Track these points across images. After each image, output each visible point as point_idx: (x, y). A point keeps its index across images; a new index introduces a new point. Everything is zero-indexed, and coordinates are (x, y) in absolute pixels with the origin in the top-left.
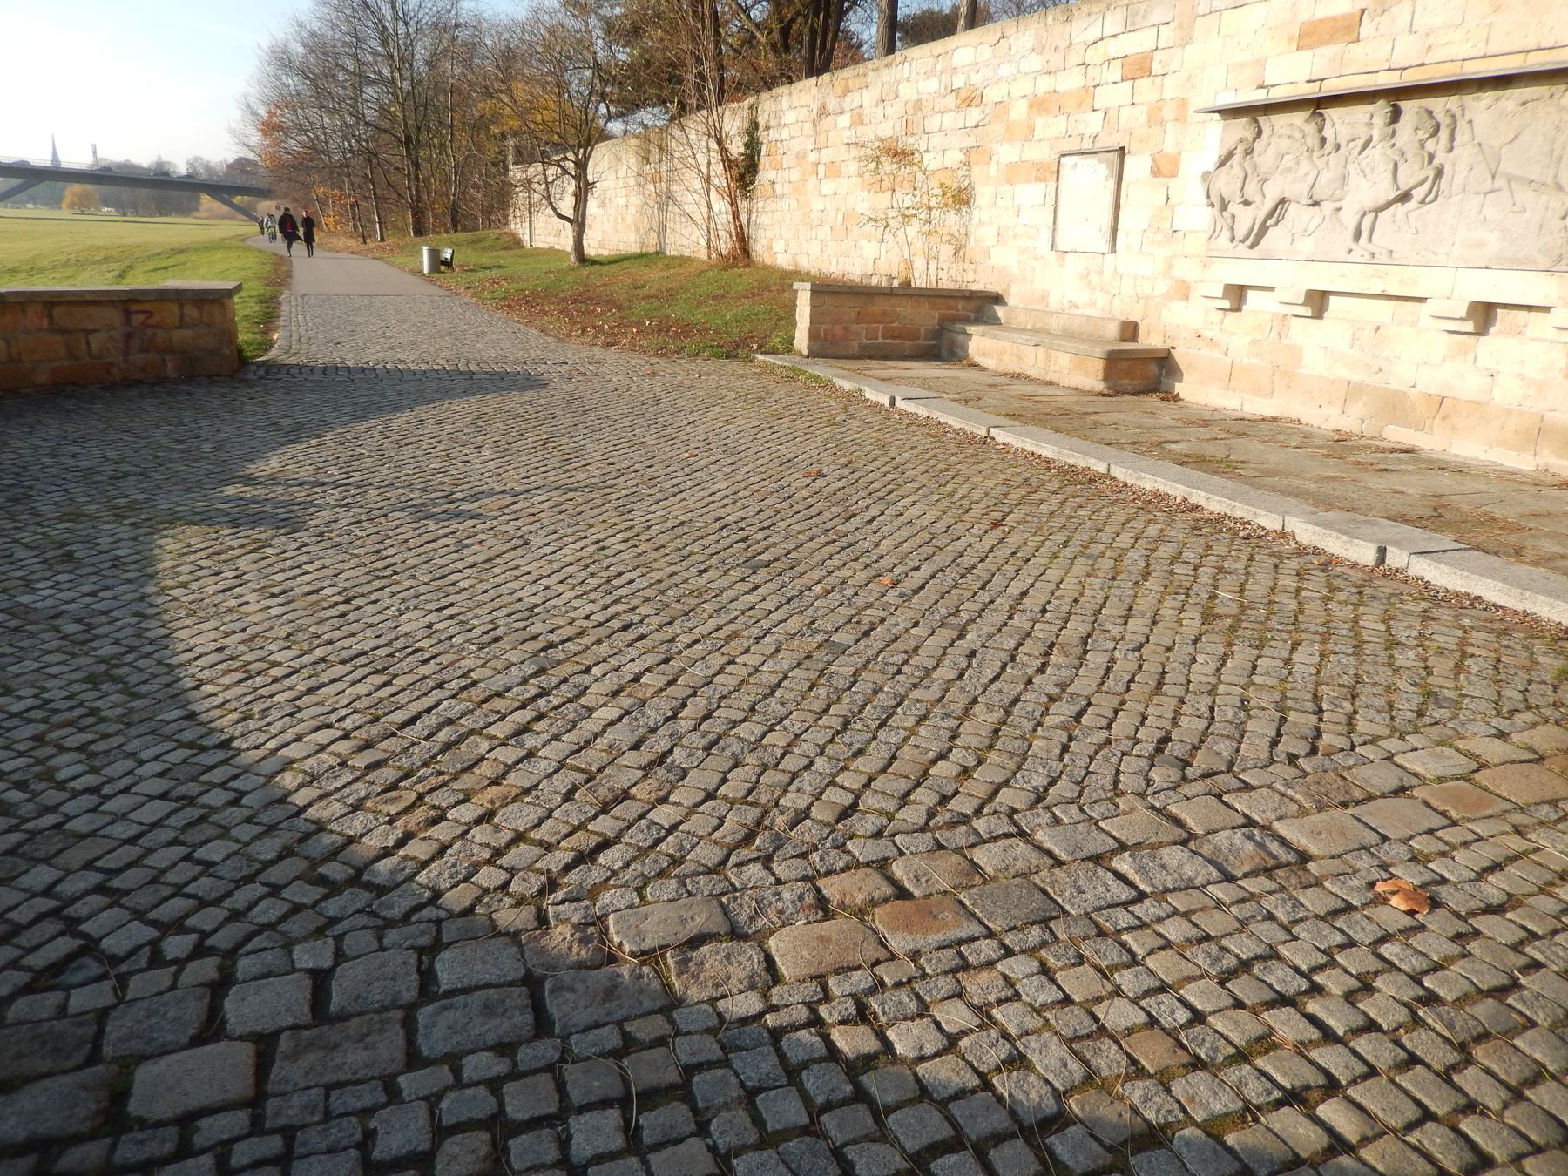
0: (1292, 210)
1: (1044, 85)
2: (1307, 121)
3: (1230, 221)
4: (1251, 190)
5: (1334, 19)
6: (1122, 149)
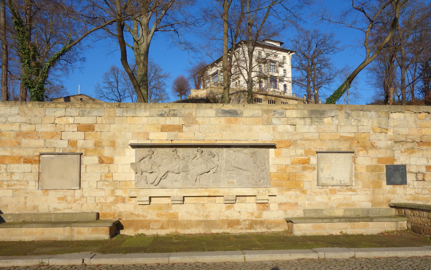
0: (170, 174)
3: (145, 178)
4: (155, 168)
5: (174, 125)
6: (81, 154)
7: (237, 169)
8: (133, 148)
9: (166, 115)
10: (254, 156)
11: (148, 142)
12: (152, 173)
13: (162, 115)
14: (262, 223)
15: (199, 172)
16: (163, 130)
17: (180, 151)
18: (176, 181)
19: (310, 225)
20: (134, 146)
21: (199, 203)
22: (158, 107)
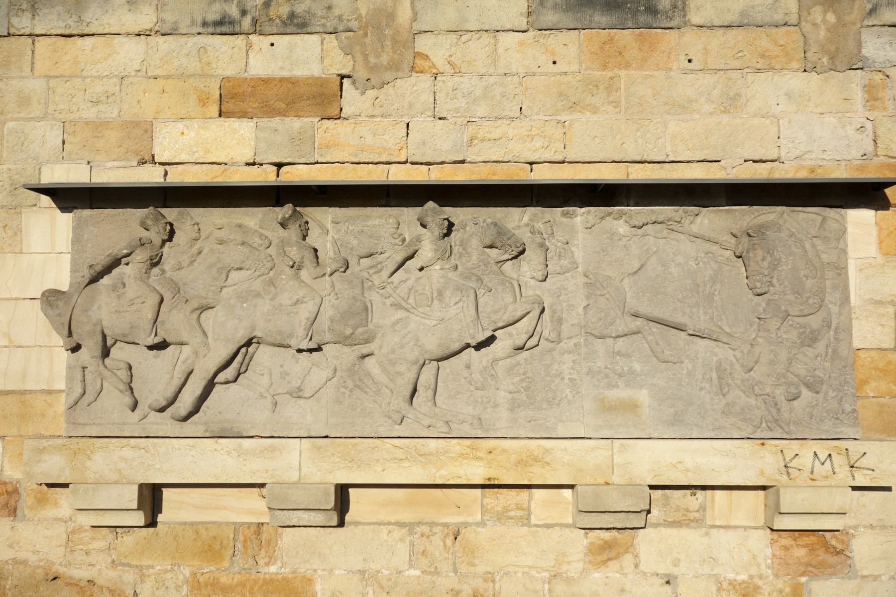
0: (263, 355)
2: (283, 225)
3: (123, 374)
4: (176, 322)
5: (292, 82)
7: (655, 328)
8: (64, 209)
9: (247, 23)
10: (760, 253)
11: (151, 176)
12: (162, 346)
15: (433, 345)
16: (227, 106)
17: (324, 220)
18: (297, 394)
20: (67, 197)
21: (432, 524)
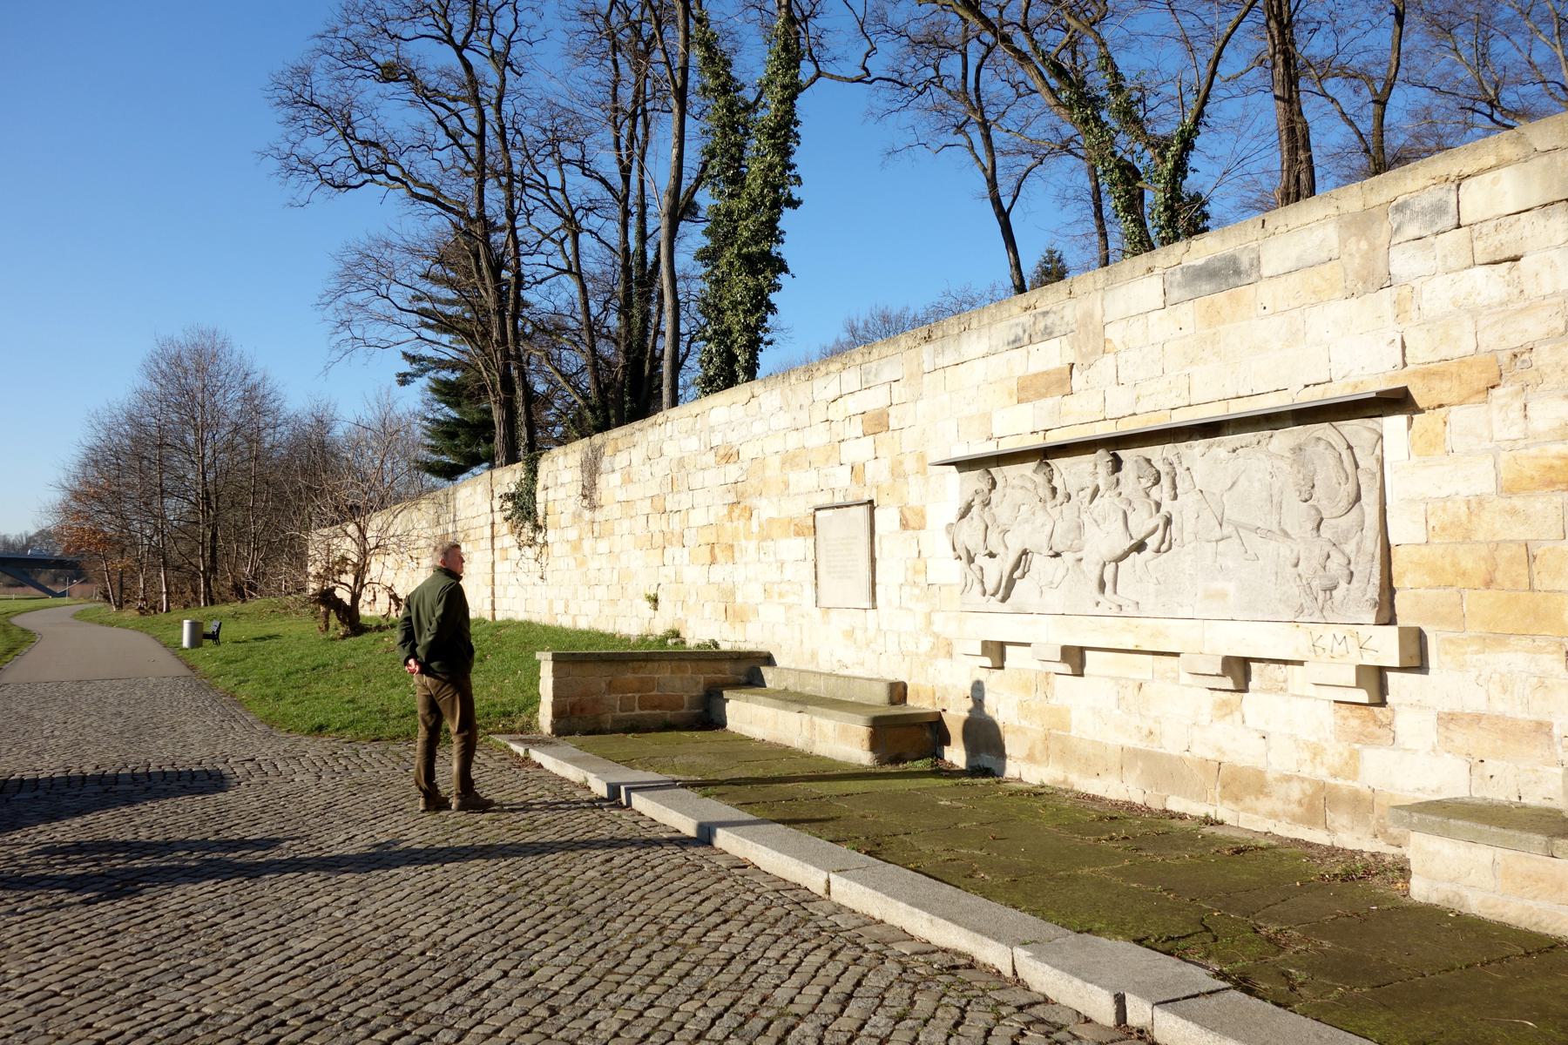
1: (793, 441)
3: (978, 573)
4: (994, 543)
6: (871, 502)
13: (1016, 343)
14: (1360, 805)
19: (1483, 854)
20: (964, 465)
22: (1005, 314)
